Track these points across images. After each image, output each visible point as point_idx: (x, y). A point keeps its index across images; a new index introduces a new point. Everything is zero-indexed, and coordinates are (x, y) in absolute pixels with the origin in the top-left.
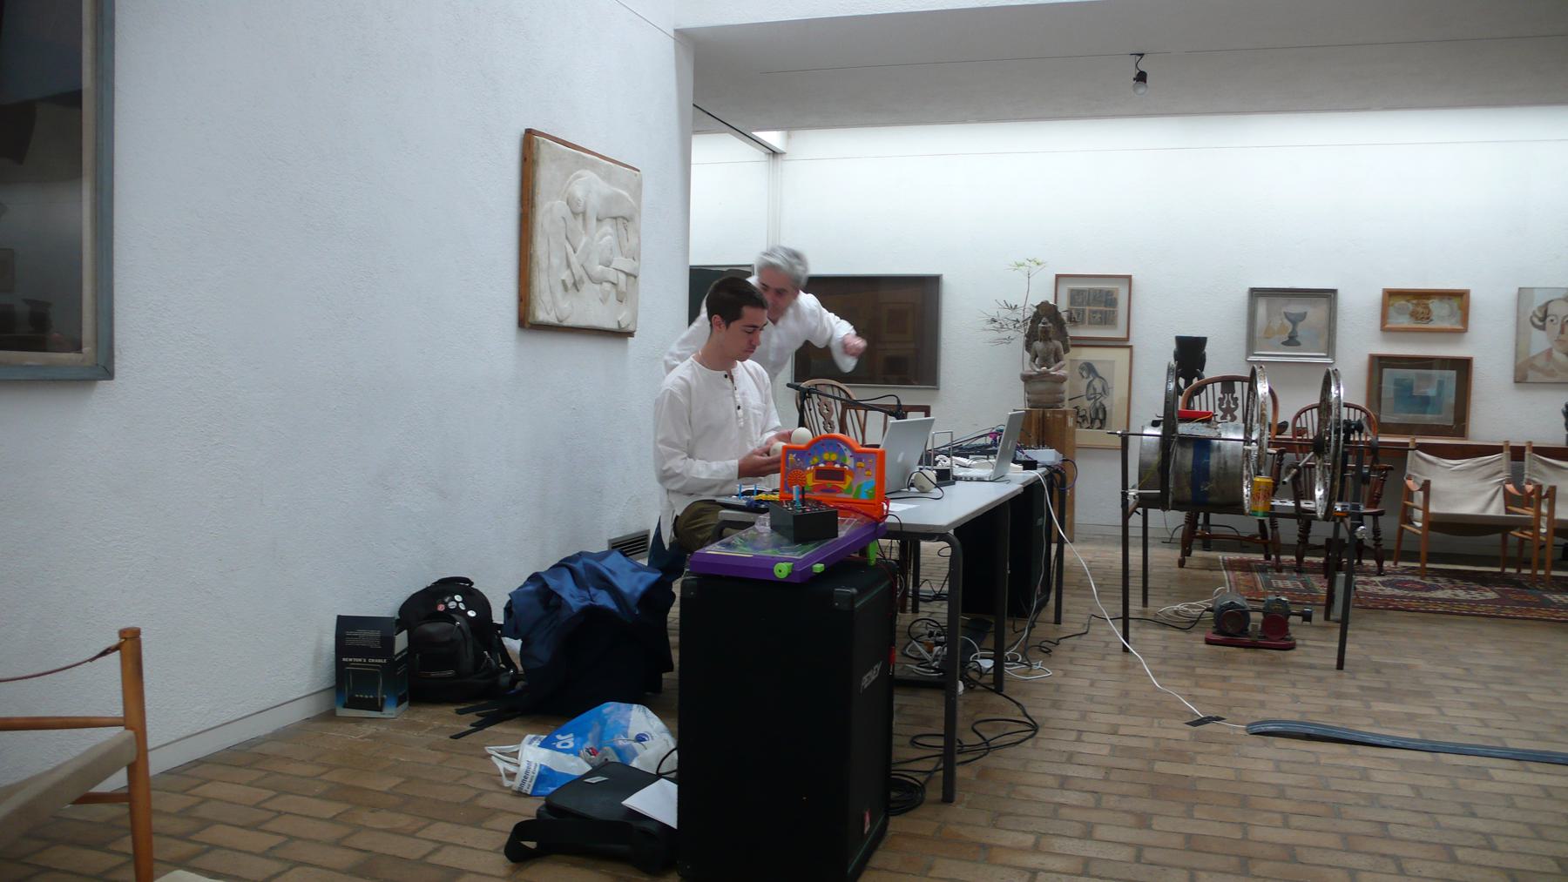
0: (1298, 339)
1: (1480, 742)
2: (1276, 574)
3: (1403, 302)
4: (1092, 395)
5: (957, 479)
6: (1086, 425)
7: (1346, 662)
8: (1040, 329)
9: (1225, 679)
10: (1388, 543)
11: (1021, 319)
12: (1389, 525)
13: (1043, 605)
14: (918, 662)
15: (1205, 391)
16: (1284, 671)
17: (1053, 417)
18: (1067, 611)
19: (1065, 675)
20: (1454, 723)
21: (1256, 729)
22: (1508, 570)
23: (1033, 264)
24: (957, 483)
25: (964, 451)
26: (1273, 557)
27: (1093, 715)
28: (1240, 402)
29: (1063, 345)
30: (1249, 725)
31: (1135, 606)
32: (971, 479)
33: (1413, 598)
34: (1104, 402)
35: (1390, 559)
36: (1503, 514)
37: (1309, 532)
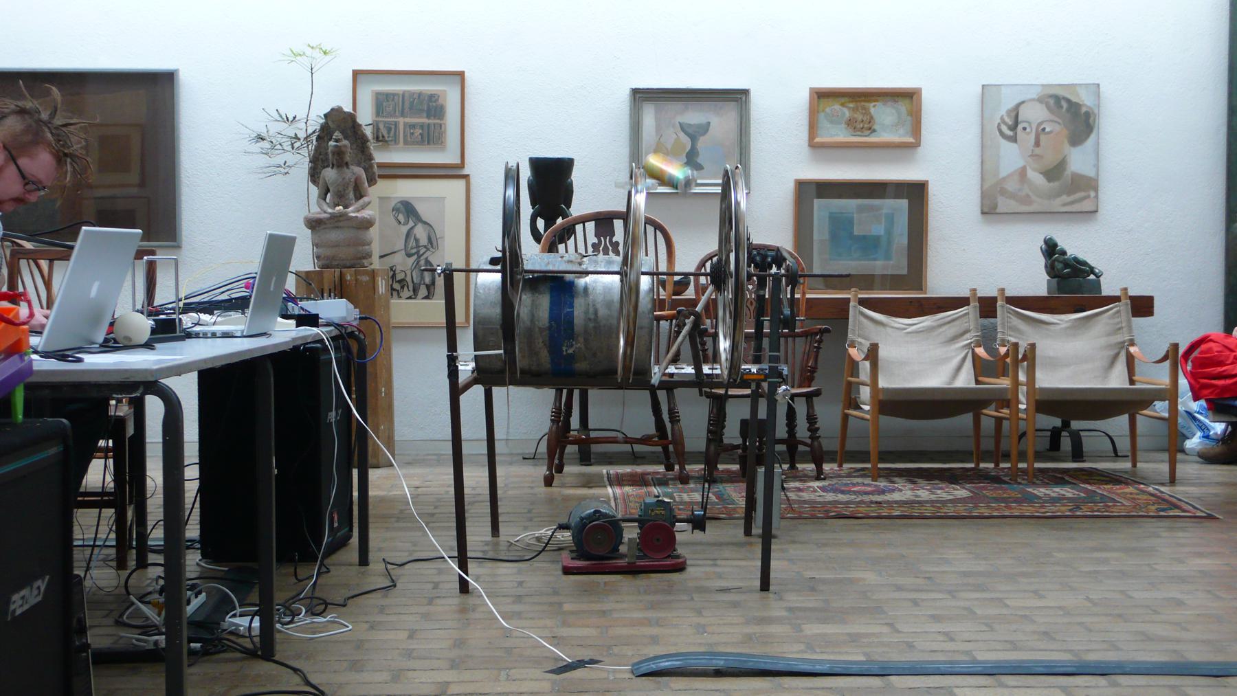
0: (700, 160)
1: (941, 658)
2: (680, 486)
3: (837, 107)
4: (414, 250)
5: (188, 335)
6: (406, 293)
7: (772, 581)
8: (330, 149)
9: (604, 613)
10: (829, 442)
11: (302, 135)
12: (828, 414)
13: (340, 544)
14: (139, 631)
15: (573, 236)
16: (685, 597)
17: (356, 280)
18: (380, 550)
19: (372, 628)
20: (911, 640)
21: (645, 668)
22: (982, 465)
23: (317, 54)
24: (188, 341)
25: (208, 307)
26: (677, 467)
27: (410, 674)
28: (621, 248)
29: (366, 170)
30: (633, 665)
31: (478, 534)
32: (214, 335)
33: (862, 502)
34: (430, 259)
35: (833, 461)
36: (973, 385)
37: (724, 427)
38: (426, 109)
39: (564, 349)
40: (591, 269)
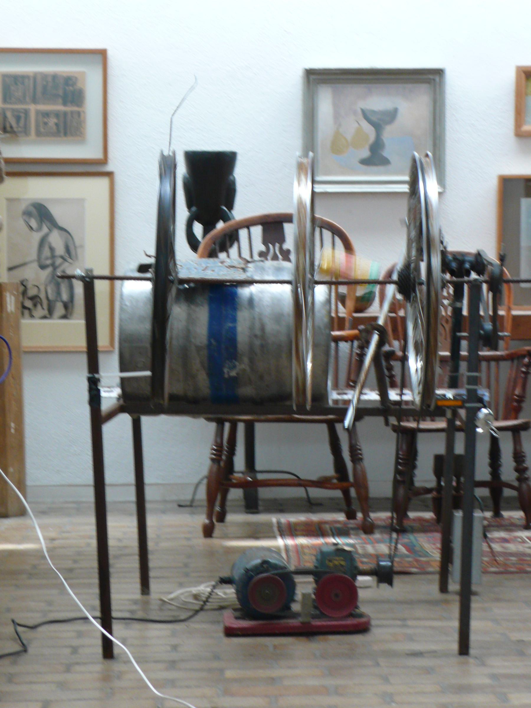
0: (386, 153)
2: (364, 536)
6: (40, 311)
15: (235, 246)
26: (360, 515)
28: (293, 257)
37: (414, 467)
38: (61, 92)
39: (226, 370)
40: (257, 278)
